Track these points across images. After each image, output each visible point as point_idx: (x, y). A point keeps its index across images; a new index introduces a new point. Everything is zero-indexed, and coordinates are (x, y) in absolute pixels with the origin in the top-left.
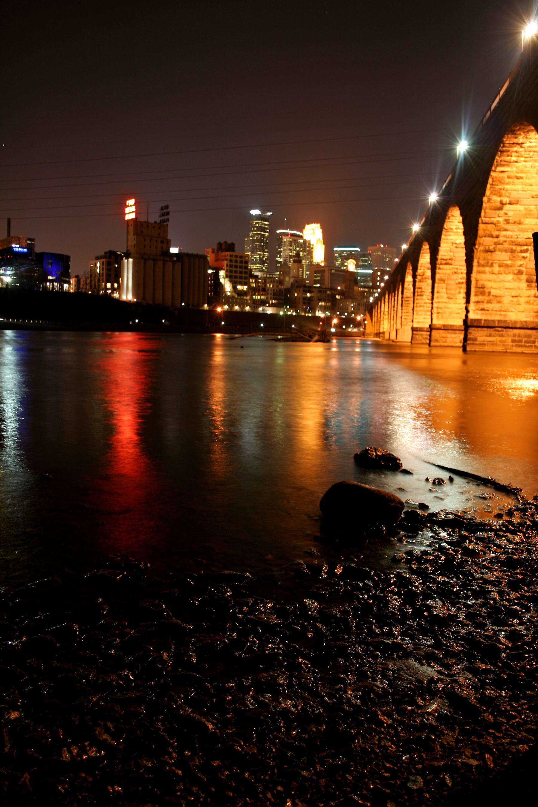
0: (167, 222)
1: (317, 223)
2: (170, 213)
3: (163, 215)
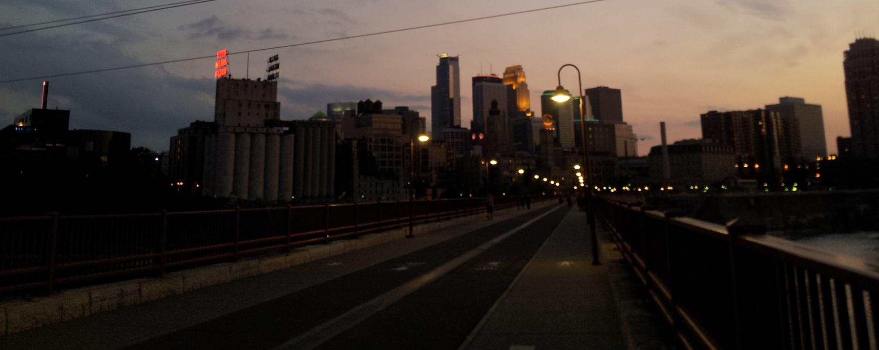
0: (276, 78)
1: (437, 84)
2: (280, 66)
3: (271, 69)
